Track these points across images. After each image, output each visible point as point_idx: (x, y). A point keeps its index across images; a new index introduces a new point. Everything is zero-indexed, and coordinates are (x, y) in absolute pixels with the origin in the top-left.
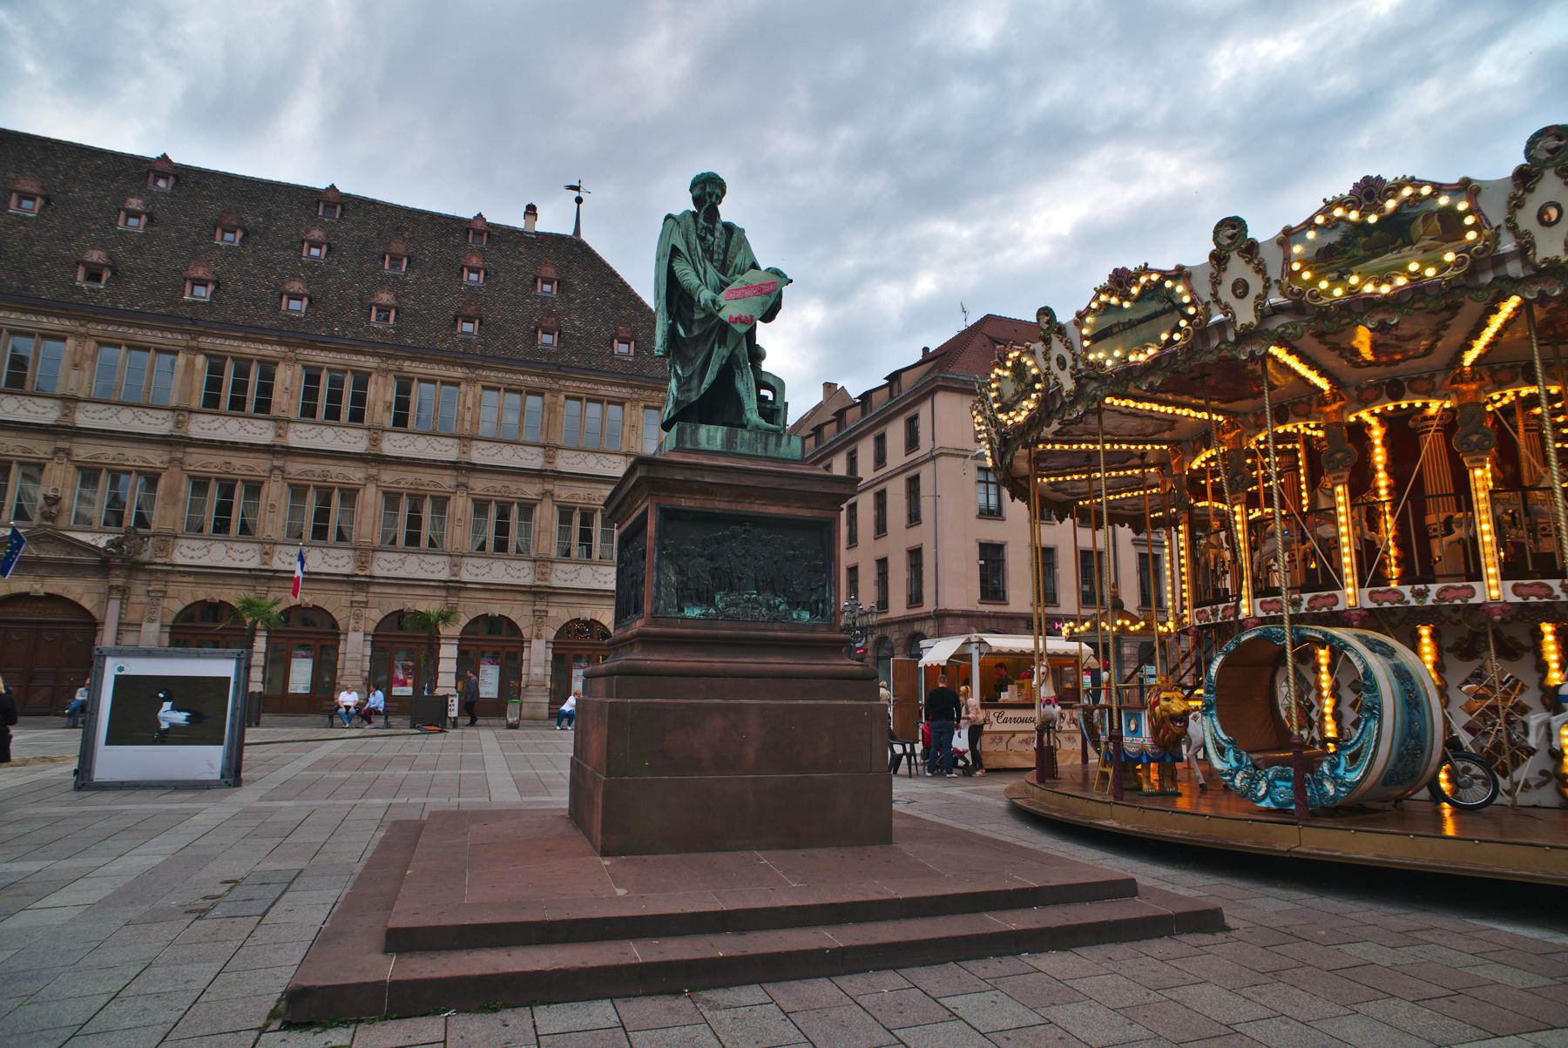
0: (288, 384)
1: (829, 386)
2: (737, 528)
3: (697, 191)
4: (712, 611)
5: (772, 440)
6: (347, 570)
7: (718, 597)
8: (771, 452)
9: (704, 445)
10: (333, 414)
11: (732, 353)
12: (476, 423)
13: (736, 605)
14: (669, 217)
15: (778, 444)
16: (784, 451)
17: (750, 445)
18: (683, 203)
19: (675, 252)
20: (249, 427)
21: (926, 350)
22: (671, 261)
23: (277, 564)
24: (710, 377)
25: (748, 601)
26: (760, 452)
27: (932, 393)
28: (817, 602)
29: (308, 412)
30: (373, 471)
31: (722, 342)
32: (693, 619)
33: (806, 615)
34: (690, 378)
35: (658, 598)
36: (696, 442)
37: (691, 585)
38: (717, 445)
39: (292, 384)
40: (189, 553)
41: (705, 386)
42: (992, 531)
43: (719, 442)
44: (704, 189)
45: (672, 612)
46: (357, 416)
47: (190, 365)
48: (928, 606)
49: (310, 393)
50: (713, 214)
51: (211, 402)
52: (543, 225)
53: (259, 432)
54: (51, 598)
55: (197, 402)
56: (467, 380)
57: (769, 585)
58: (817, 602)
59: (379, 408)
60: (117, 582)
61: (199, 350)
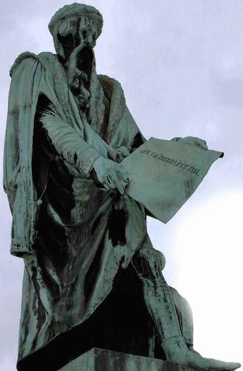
3: (65, 28)
14: (26, 57)
18: (44, 43)
19: (43, 103)
22: (38, 116)
24: (103, 288)
31: (119, 238)
41: (96, 301)
44: (78, 24)
50: (87, 59)
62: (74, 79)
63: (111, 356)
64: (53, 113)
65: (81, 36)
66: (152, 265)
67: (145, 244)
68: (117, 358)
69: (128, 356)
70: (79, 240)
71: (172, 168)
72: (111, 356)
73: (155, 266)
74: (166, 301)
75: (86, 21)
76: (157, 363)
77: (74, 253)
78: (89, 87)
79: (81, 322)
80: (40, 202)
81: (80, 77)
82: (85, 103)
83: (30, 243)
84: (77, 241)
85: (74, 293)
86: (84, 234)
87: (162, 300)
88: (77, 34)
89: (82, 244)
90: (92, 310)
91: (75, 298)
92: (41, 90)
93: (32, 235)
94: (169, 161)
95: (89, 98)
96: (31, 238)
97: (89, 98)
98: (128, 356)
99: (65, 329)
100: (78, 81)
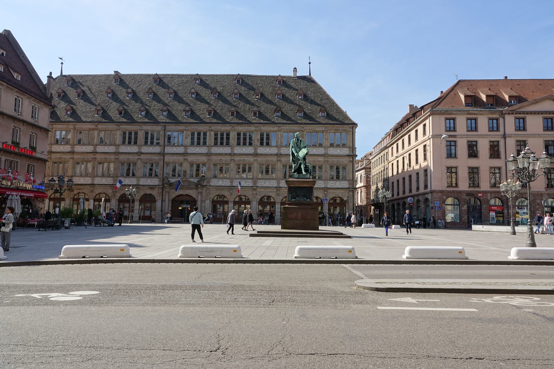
1: (411, 106)
6: (251, 185)
10: (245, 144)
12: (281, 142)
21: (442, 92)
23: (234, 185)
27: (429, 116)
29: (239, 144)
30: (256, 158)
40: (214, 182)
42: (452, 162)
46: (250, 144)
47: (210, 134)
48: (429, 189)
49: (239, 139)
51: (216, 144)
52: (299, 74)
53: (227, 150)
54: (187, 195)
55: (213, 144)
56: (279, 131)
57: (304, 196)
59: (256, 141)
60: (200, 190)
61: (212, 130)
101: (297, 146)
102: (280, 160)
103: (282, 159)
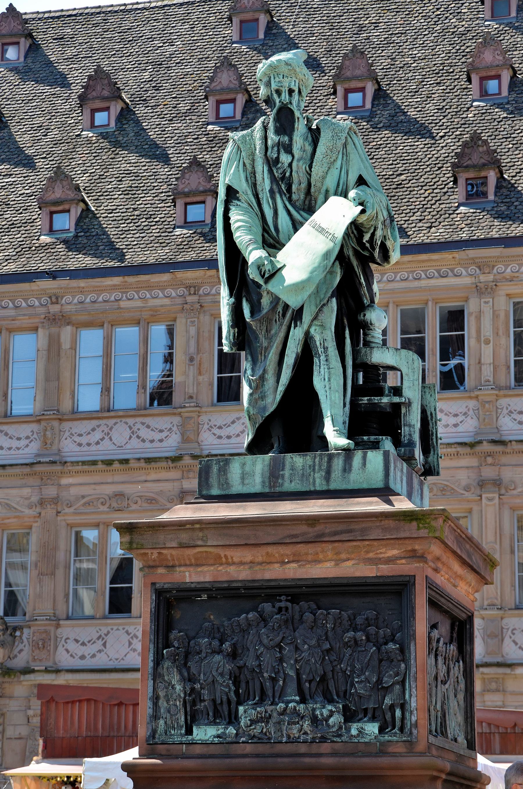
0: (192, 349)
2: (267, 607)
4: (232, 730)
5: (338, 464)
7: (241, 709)
8: (337, 483)
9: (237, 488)
11: (307, 334)
13: (267, 719)
15: (347, 469)
16: (356, 479)
17: (304, 477)
20: (144, 433)
22: (226, 211)
25: (283, 712)
26: (320, 485)
28: (392, 708)
32: (204, 743)
33: (372, 728)
34: (262, 378)
35: (155, 717)
36: (227, 484)
37: (206, 694)
38: (256, 485)
39: (198, 351)
41: (281, 388)
43: (258, 479)
45: (177, 735)
58: (392, 708)
62: (273, 147)
63: (216, 464)
64: (239, 203)
65: (275, 96)
66: (318, 343)
67: (315, 322)
68: (221, 463)
69: (233, 459)
70: (268, 329)
71: (321, 237)
72: (216, 464)
73: (321, 344)
74: (324, 379)
75: (274, 78)
76: (264, 461)
77: (265, 344)
78: (292, 149)
79: (271, 409)
80: (233, 300)
81: (278, 144)
82: (284, 173)
83: (230, 342)
84: (267, 331)
85: (265, 383)
86: (274, 321)
87: (323, 379)
88: (272, 94)
89: (273, 332)
90: (278, 397)
91: (266, 387)
92: (227, 181)
93: (232, 334)
94: (321, 230)
95: (290, 165)
96: (231, 337)
97: (290, 165)
98: (233, 459)
99: (260, 420)
100: (276, 149)
101: (282, 183)
102: (497, 483)
103: (507, 474)
